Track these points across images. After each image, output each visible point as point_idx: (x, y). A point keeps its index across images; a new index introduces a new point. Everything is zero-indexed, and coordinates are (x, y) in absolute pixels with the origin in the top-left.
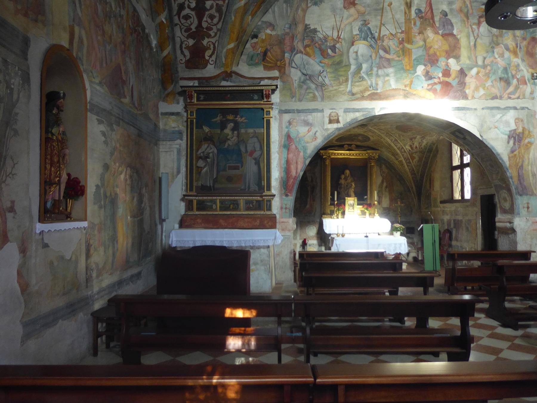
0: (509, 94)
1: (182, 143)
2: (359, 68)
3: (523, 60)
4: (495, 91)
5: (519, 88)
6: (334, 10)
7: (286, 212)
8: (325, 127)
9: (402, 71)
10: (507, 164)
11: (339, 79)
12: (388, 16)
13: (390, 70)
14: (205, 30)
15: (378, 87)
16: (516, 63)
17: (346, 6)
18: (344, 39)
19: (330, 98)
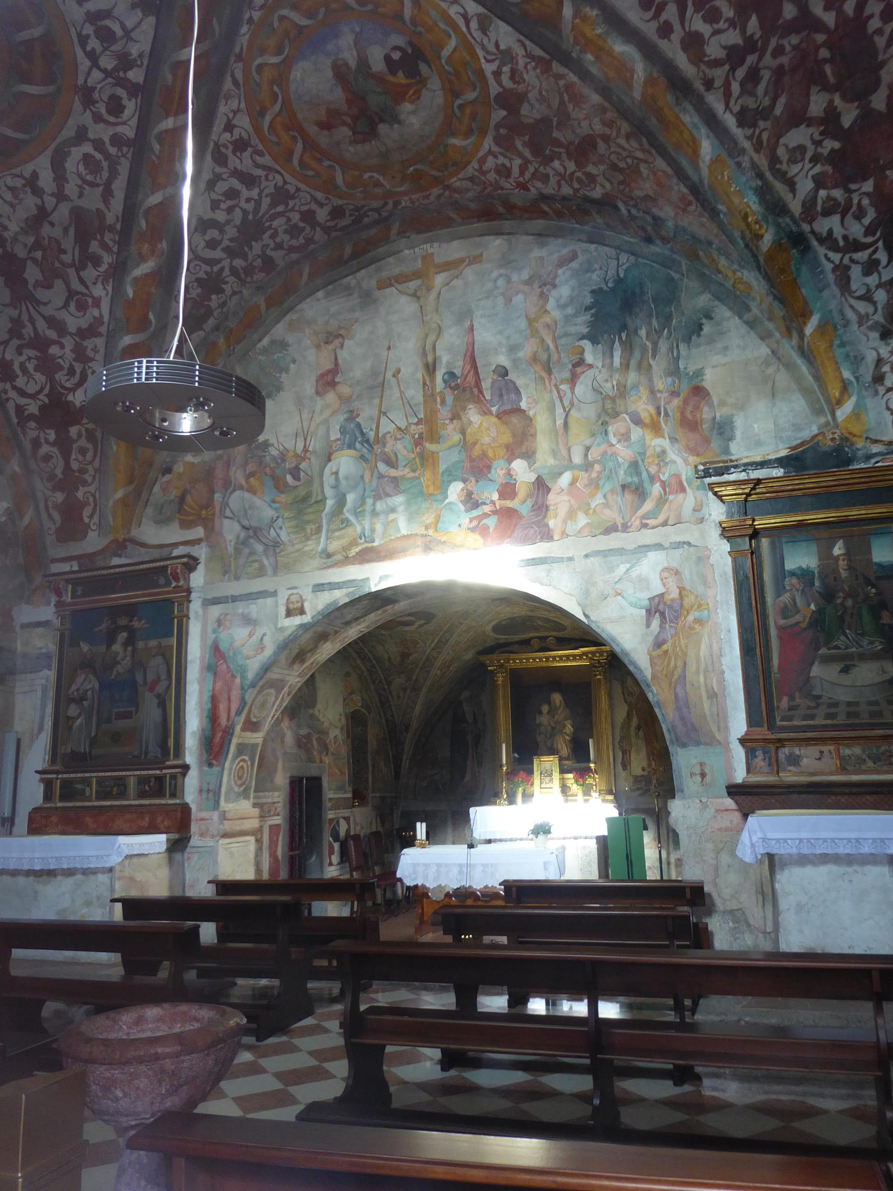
0: (643, 517)
1: (50, 675)
2: (341, 502)
3: (673, 440)
4: (612, 515)
5: (667, 500)
6: (299, 402)
7: (208, 799)
8: (279, 625)
9: (420, 499)
10: (648, 674)
11: (304, 529)
12: (393, 394)
13: (399, 499)
14: (77, 474)
15: (375, 536)
16: (658, 449)
17: (320, 390)
18: (315, 452)
19: (289, 568)
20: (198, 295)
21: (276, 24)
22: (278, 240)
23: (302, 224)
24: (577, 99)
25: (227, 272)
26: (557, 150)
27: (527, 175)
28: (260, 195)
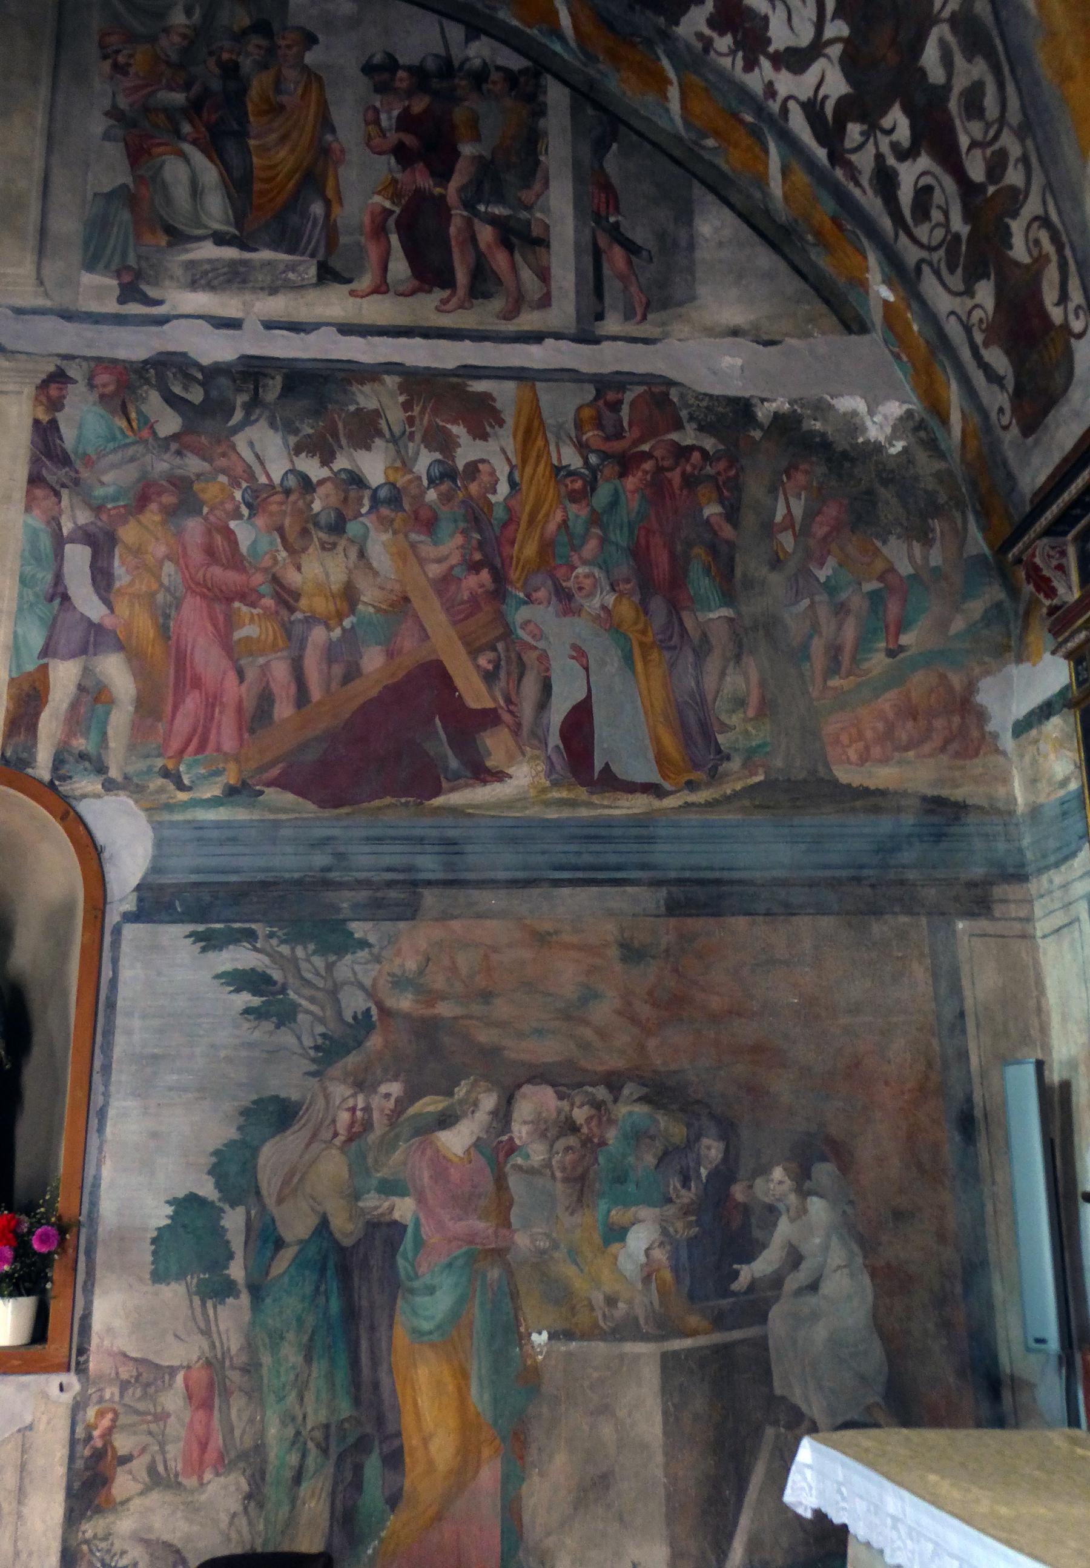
14: (991, 190)
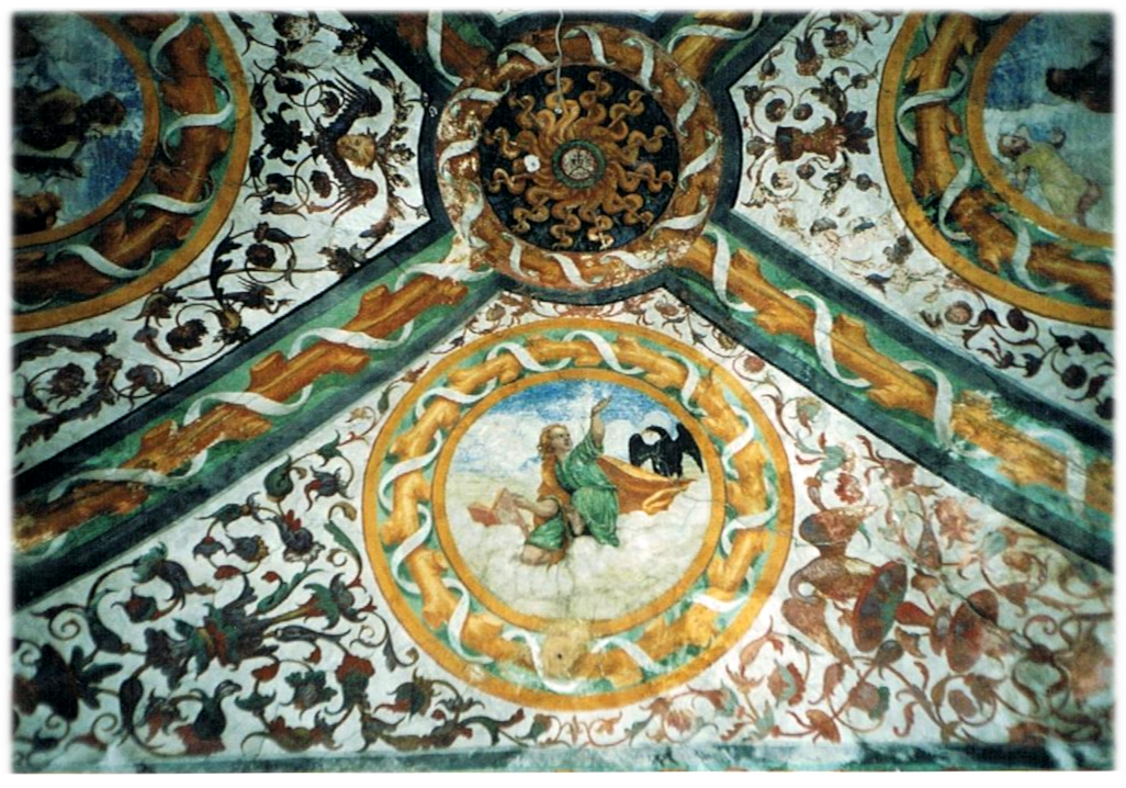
20: (18, 679)
21: (491, 356)
22: (266, 688)
23: (332, 682)
24: (954, 528)
25: (114, 682)
26: (910, 629)
27: (841, 693)
28: (298, 579)
